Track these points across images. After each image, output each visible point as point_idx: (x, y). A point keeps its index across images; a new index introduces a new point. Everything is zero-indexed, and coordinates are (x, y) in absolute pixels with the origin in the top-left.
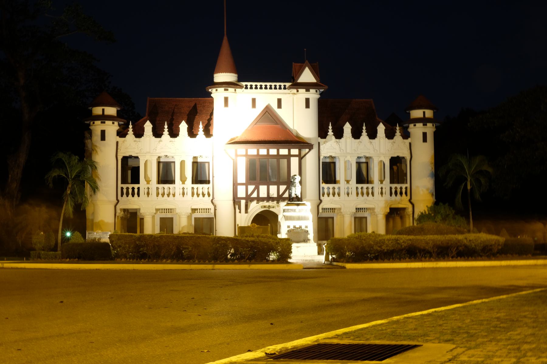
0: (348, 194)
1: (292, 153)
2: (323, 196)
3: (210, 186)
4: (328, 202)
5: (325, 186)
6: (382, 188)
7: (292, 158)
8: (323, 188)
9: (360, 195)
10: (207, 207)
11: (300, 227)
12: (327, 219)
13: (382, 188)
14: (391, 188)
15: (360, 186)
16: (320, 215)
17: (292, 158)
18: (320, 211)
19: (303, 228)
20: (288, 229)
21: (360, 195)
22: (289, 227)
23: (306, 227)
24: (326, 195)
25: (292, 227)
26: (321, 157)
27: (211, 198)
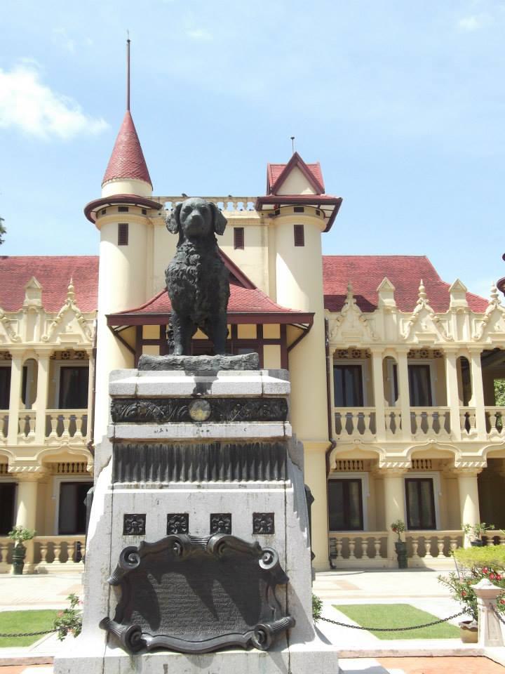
0: (393, 427)
1: (266, 336)
2: (338, 432)
3: (89, 411)
4: (350, 446)
5: (344, 411)
6: (467, 415)
7: (267, 348)
8: (338, 415)
9: (419, 430)
10: (80, 461)
11: (221, 522)
12: (346, 483)
13: (467, 415)
14: (487, 415)
15: (419, 410)
16: (333, 476)
17: (267, 348)
18: (333, 465)
19: (242, 529)
20: (135, 541)
21: (419, 430)
22: (134, 524)
23: (264, 523)
24: (344, 432)
25: (156, 531)
26: (332, 350)
27: (89, 440)
